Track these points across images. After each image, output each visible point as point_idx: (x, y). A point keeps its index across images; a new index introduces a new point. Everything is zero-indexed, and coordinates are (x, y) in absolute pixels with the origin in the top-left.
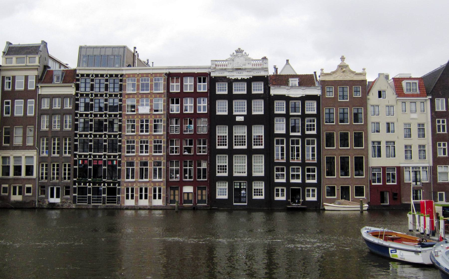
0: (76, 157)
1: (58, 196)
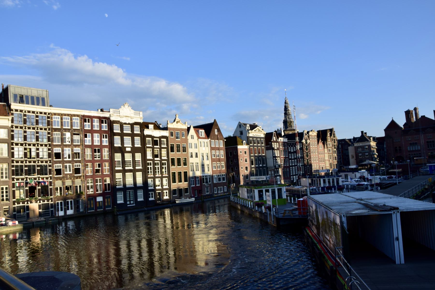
0: (13, 180)
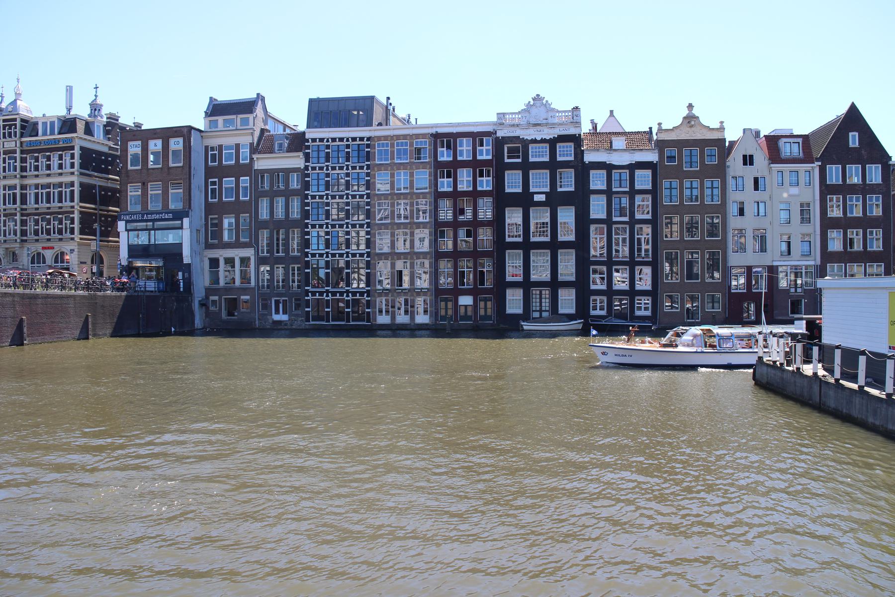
1: (285, 312)
